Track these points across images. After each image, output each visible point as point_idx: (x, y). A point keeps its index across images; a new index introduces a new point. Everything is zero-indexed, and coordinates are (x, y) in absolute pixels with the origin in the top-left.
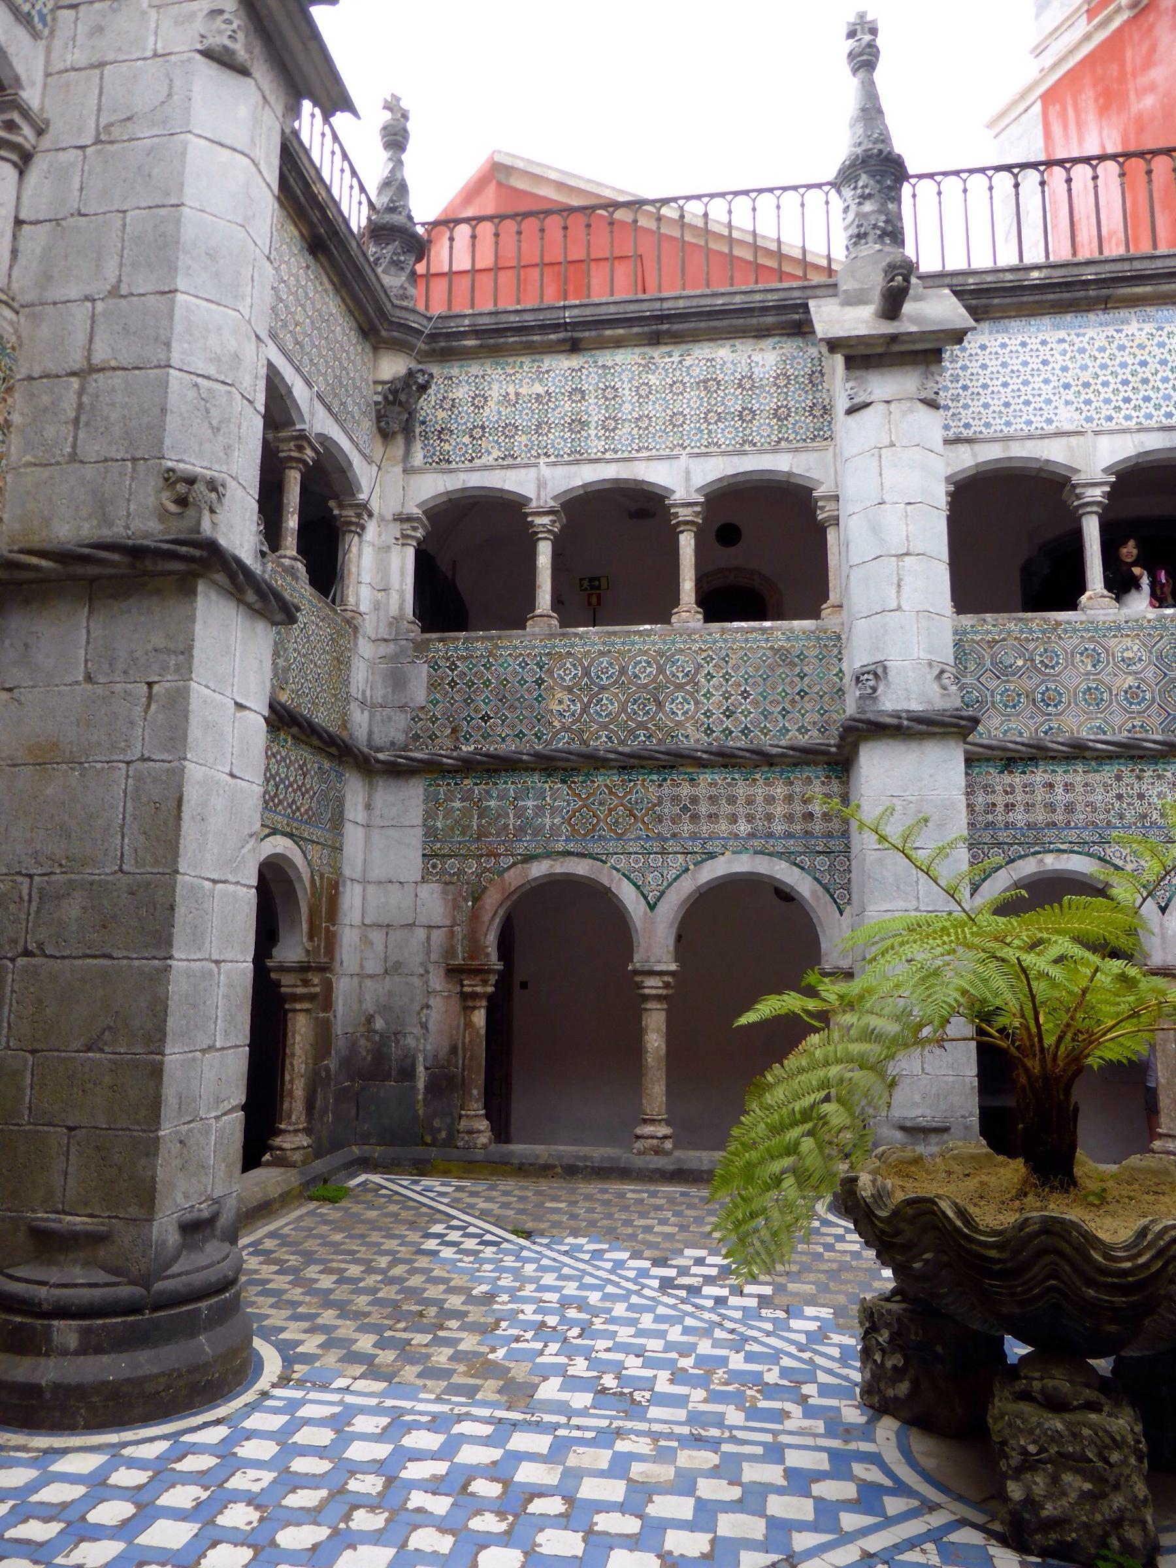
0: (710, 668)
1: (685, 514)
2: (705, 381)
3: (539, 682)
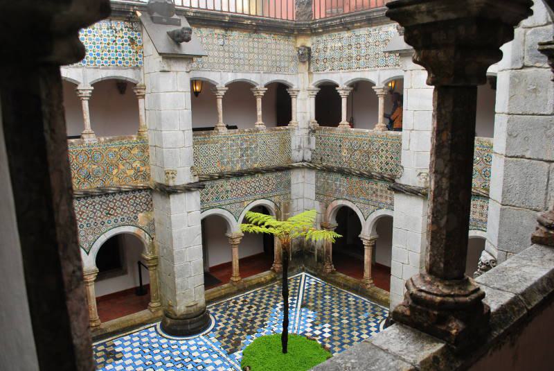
0: (382, 148)
1: (378, 92)
2: (385, 41)
3: (340, 146)
